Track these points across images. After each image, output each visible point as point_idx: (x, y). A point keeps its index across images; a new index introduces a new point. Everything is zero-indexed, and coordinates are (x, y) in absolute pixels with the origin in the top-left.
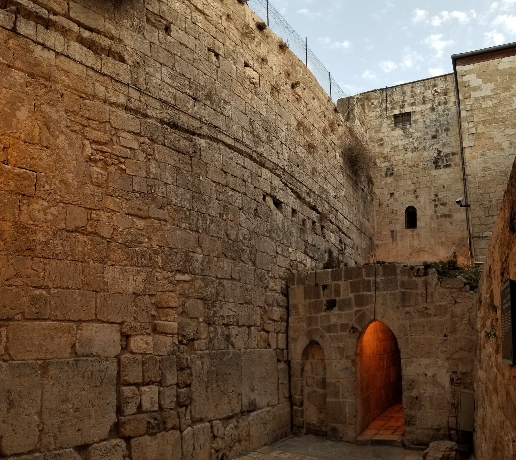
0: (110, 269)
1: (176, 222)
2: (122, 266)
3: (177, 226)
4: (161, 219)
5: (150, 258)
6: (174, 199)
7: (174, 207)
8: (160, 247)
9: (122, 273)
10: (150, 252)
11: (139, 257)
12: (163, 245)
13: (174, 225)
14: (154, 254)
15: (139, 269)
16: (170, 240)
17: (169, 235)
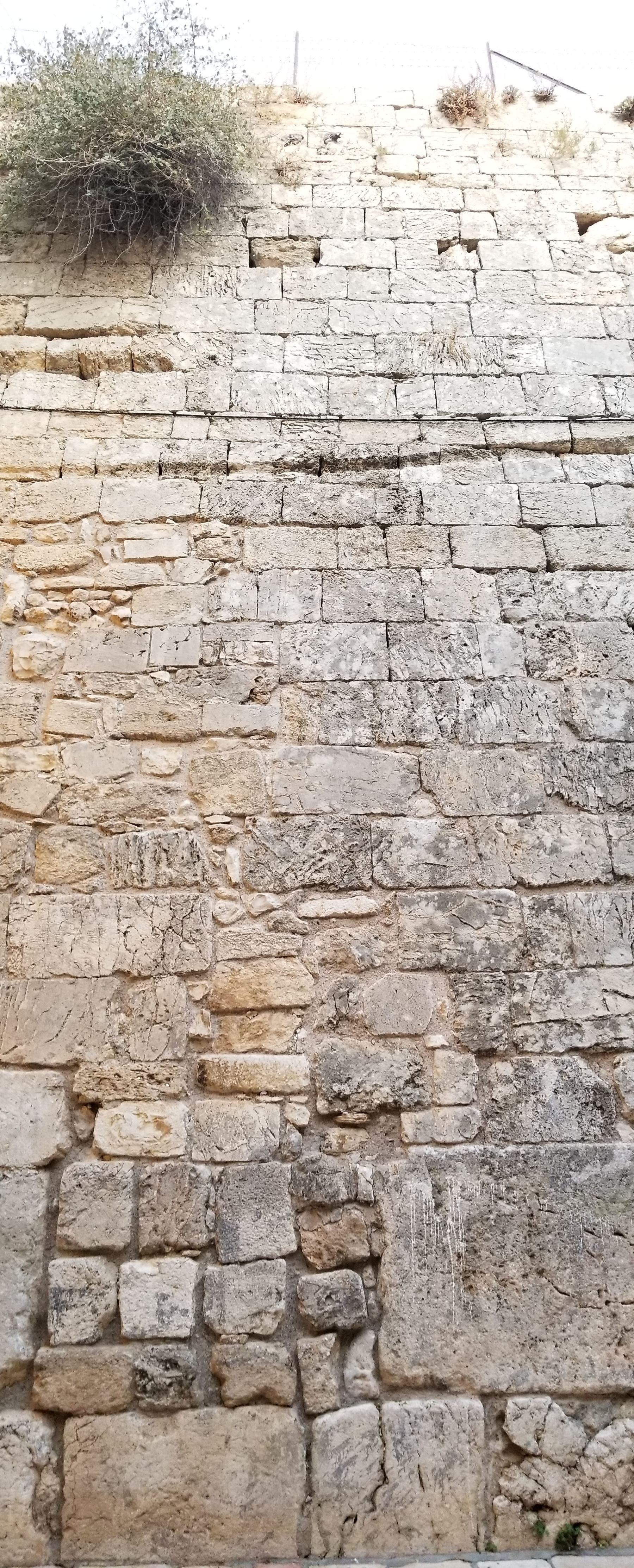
0: (32, 908)
1: (312, 731)
2: (79, 891)
3: (319, 741)
4: (247, 731)
5: (196, 856)
6: (306, 665)
7: (305, 686)
8: (242, 817)
9: (78, 913)
10: (200, 838)
11: (147, 858)
12: (249, 810)
13: (301, 740)
14: (215, 842)
15: (142, 895)
16: (281, 791)
17: (276, 778)
